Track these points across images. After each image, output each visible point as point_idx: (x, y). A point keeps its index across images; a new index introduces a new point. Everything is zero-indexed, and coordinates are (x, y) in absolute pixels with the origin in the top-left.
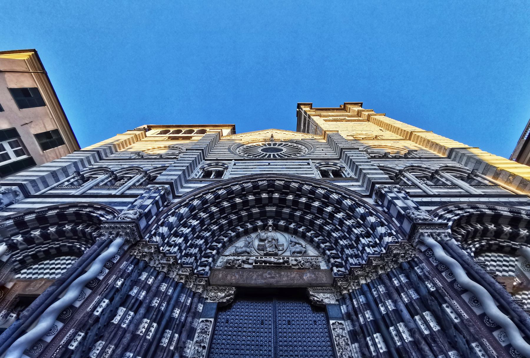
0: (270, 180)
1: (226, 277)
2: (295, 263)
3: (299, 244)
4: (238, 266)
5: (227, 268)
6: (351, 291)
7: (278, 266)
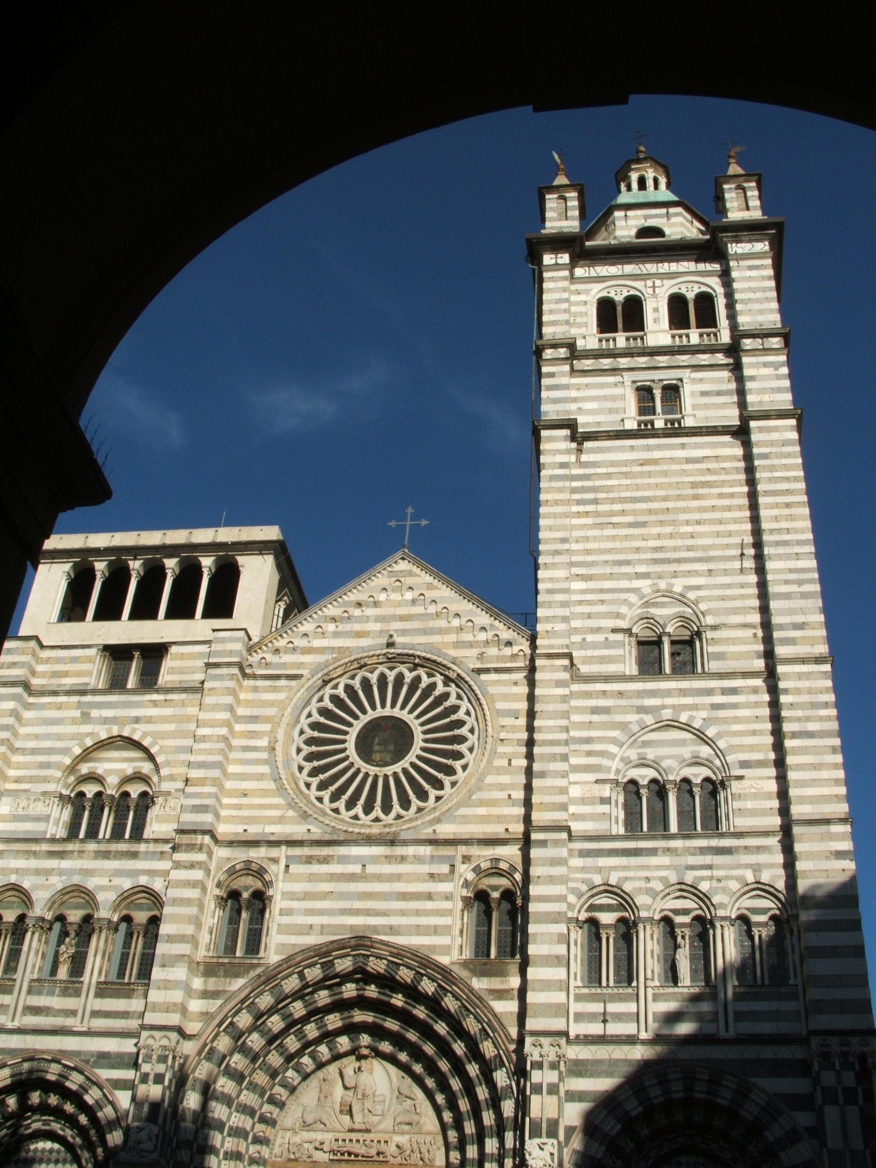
0: (357, 955)
5: (290, 1160)
7: (368, 1159)
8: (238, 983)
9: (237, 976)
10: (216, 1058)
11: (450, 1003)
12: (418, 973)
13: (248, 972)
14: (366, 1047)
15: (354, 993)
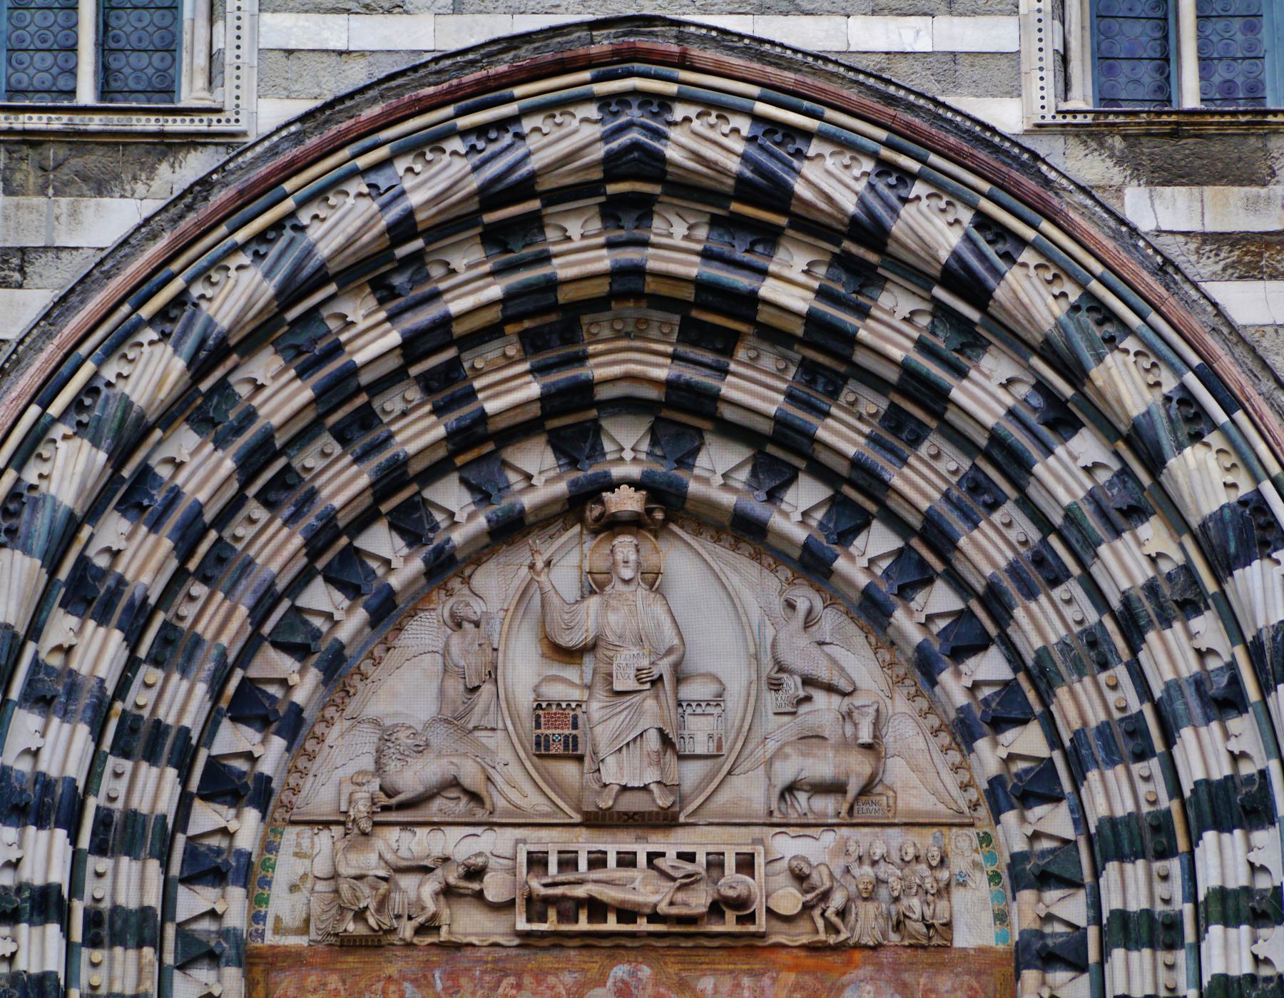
0: (622, 98)
2: (789, 899)
3: (830, 688)
4: (421, 930)
5: (347, 944)
8: (108, 219)
9: (101, 188)
10: (40, 526)
11: (1031, 294)
12: (886, 168)
13: (153, 169)
14: (636, 485)
15: (604, 261)
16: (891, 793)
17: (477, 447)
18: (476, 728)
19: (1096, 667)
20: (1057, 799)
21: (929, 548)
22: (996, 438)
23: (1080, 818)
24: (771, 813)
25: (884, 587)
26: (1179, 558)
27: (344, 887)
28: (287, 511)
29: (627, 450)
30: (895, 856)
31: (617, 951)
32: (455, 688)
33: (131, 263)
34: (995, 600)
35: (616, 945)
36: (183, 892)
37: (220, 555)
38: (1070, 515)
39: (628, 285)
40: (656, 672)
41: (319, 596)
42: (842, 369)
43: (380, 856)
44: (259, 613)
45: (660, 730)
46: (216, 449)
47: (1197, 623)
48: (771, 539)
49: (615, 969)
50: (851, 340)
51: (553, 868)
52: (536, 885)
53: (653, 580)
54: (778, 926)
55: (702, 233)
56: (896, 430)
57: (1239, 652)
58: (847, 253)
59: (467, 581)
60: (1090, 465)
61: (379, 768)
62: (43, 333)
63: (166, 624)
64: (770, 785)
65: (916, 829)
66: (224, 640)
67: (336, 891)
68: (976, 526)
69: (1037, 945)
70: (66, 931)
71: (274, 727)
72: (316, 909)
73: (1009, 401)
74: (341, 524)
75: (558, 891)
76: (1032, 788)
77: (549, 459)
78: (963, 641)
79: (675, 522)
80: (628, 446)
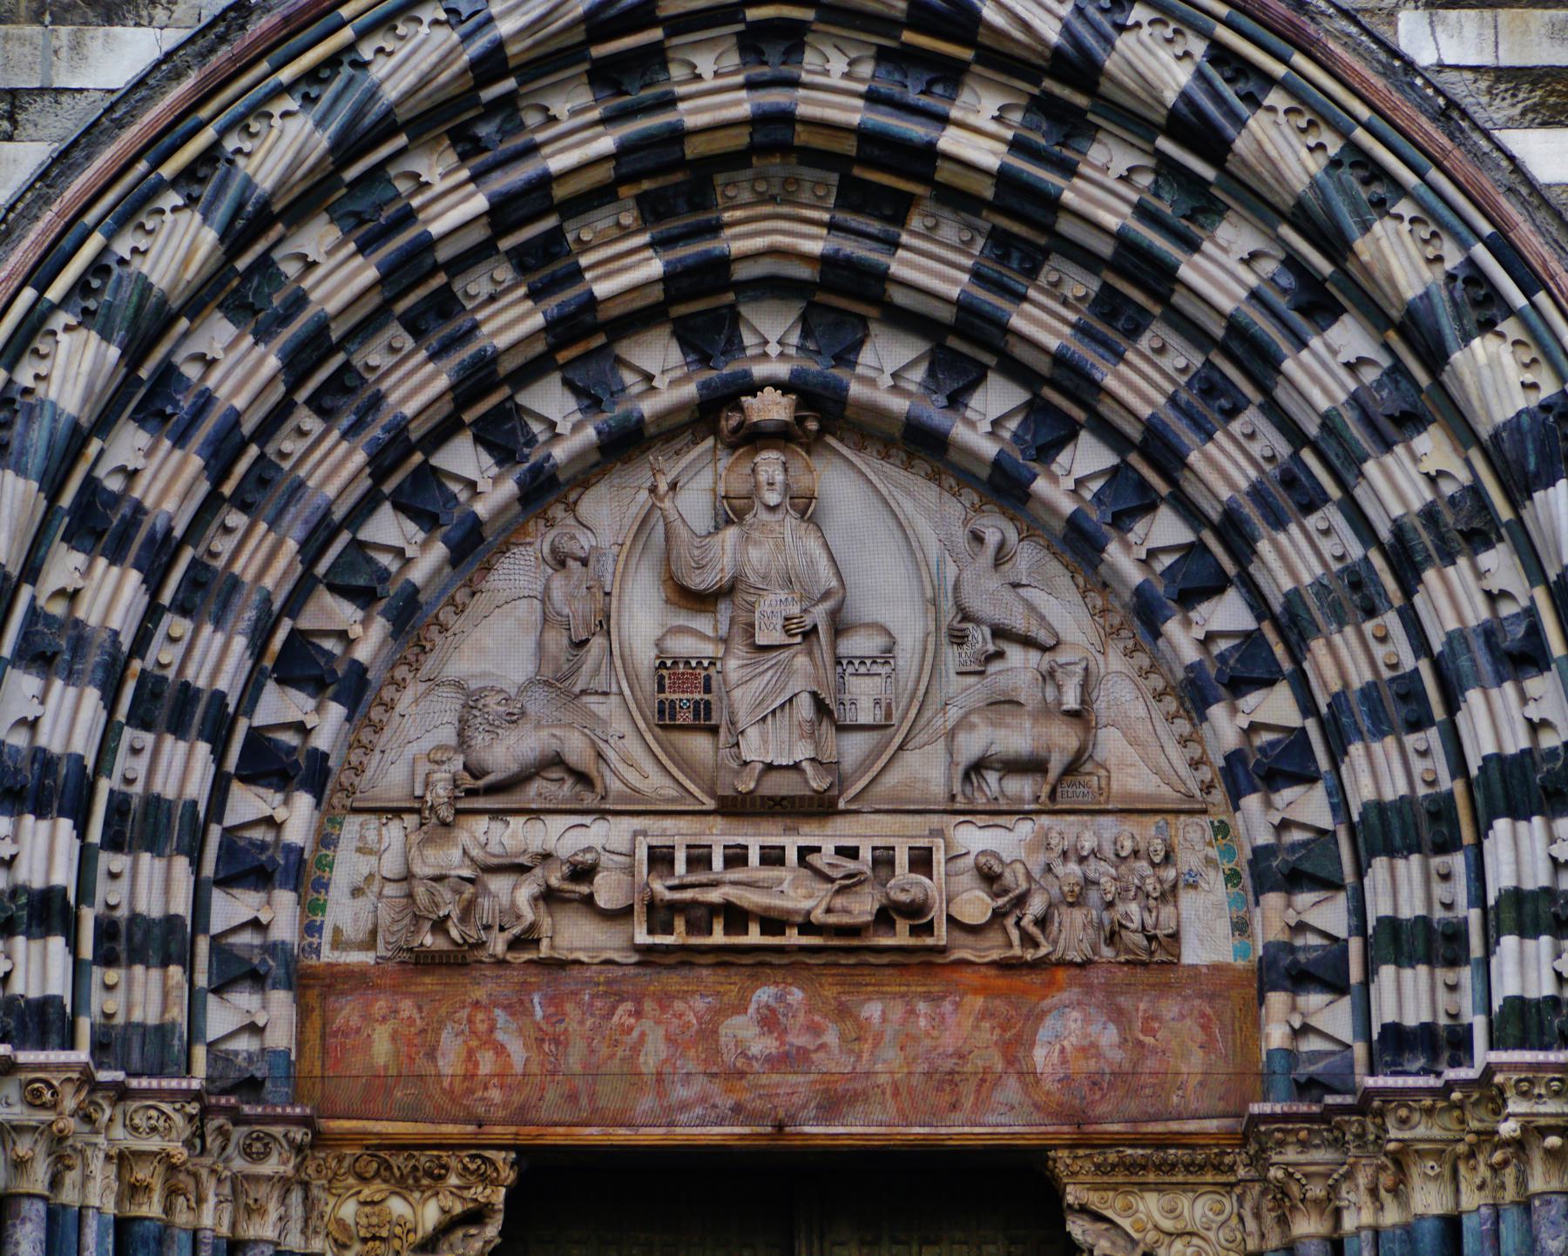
1: (431, 1055)
2: (975, 905)
3: (1027, 642)
4: (515, 944)
5: (423, 962)
6: (1349, 1223)
14: (784, 387)
15: (742, 105)
16: (1103, 773)
17: (584, 340)
18: (583, 692)
19: (1360, 614)
20: (1310, 779)
21: (1151, 464)
22: (1235, 326)
23: (1340, 804)
24: (953, 797)
25: (1095, 515)
26: (1464, 477)
27: (420, 891)
28: (346, 421)
29: (772, 343)
30: (1108, 851)
31: (760, 970)
32: (557, 641)
33: (149, 109)
34: (1234, 532)
35: (759, 962)
36: (218, 898)
37: (263, 475)
38: (1329, 423)
39: (773, 135)
40: (808, 622)
41: (387, 527)
42: (1042, 241)
43: (465, 852)
44: (311, 549)
45: (814, 695)
46: (256, 343)
47: (1487, 559)
48: (953, 455)
49: (758, 992)
50: (1053, 204)
51: (680, 867)
52: (658, 886)
53: (805, 507)
54: (961, 937)
55: (866, 69)
56: (1109, 318)
57: (1540, 595)
58: (1049, 95)
59: (571, 508)
60: (1353, 360)
61: (463, 742)
62: (40, 196)
63: (194, 562)
64: (952, 763)
65: (1135, 817)
66: (269, 582)
67: (410, 896)
68: (1210, 437)
69: (1286, 960)
70: (73, 946)
71: (331, 691)
72: (385, 917)
73: (1252, 281)
74: (414, 437)
75: (687, 895)
76: (1279, 764)
77: (675, 355)
78: (1194, 583)
79: (833, 435)
80: (773, 338)
